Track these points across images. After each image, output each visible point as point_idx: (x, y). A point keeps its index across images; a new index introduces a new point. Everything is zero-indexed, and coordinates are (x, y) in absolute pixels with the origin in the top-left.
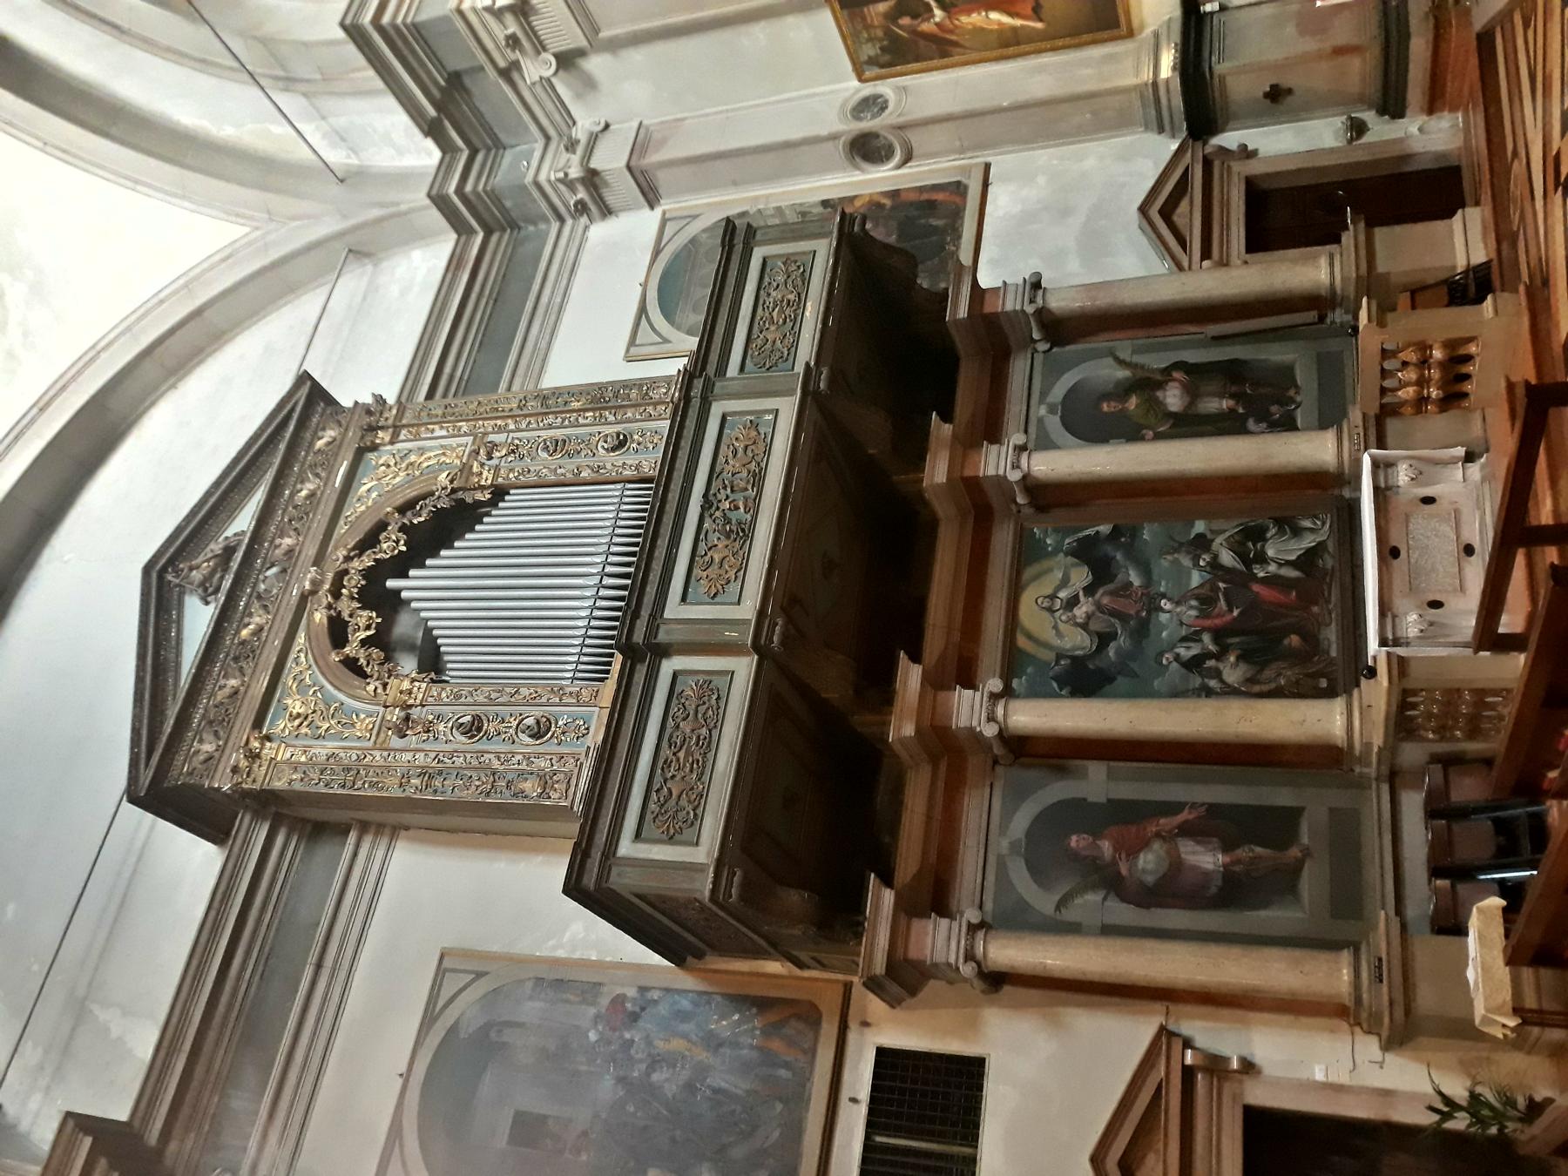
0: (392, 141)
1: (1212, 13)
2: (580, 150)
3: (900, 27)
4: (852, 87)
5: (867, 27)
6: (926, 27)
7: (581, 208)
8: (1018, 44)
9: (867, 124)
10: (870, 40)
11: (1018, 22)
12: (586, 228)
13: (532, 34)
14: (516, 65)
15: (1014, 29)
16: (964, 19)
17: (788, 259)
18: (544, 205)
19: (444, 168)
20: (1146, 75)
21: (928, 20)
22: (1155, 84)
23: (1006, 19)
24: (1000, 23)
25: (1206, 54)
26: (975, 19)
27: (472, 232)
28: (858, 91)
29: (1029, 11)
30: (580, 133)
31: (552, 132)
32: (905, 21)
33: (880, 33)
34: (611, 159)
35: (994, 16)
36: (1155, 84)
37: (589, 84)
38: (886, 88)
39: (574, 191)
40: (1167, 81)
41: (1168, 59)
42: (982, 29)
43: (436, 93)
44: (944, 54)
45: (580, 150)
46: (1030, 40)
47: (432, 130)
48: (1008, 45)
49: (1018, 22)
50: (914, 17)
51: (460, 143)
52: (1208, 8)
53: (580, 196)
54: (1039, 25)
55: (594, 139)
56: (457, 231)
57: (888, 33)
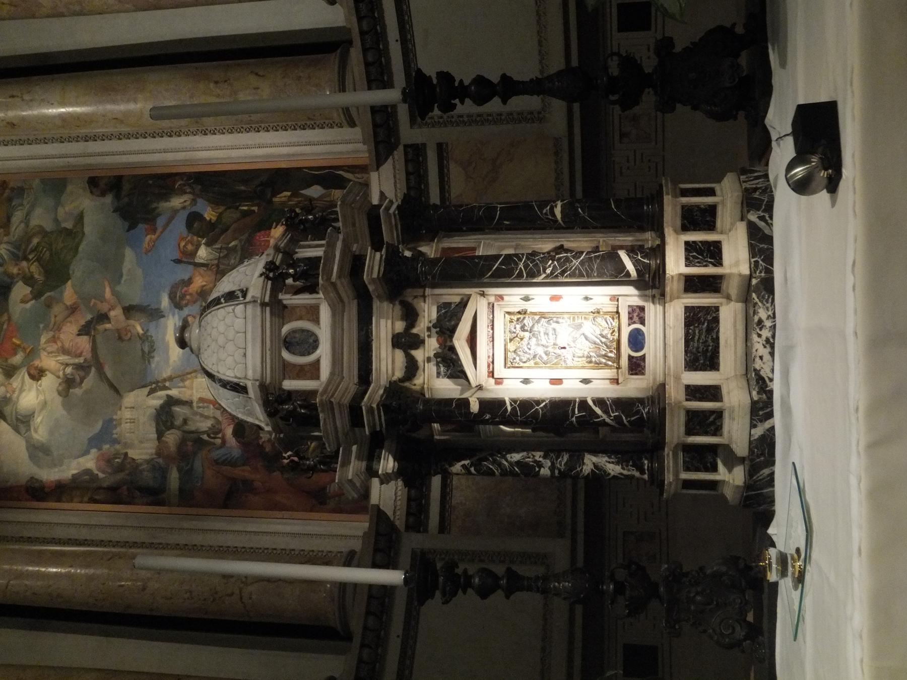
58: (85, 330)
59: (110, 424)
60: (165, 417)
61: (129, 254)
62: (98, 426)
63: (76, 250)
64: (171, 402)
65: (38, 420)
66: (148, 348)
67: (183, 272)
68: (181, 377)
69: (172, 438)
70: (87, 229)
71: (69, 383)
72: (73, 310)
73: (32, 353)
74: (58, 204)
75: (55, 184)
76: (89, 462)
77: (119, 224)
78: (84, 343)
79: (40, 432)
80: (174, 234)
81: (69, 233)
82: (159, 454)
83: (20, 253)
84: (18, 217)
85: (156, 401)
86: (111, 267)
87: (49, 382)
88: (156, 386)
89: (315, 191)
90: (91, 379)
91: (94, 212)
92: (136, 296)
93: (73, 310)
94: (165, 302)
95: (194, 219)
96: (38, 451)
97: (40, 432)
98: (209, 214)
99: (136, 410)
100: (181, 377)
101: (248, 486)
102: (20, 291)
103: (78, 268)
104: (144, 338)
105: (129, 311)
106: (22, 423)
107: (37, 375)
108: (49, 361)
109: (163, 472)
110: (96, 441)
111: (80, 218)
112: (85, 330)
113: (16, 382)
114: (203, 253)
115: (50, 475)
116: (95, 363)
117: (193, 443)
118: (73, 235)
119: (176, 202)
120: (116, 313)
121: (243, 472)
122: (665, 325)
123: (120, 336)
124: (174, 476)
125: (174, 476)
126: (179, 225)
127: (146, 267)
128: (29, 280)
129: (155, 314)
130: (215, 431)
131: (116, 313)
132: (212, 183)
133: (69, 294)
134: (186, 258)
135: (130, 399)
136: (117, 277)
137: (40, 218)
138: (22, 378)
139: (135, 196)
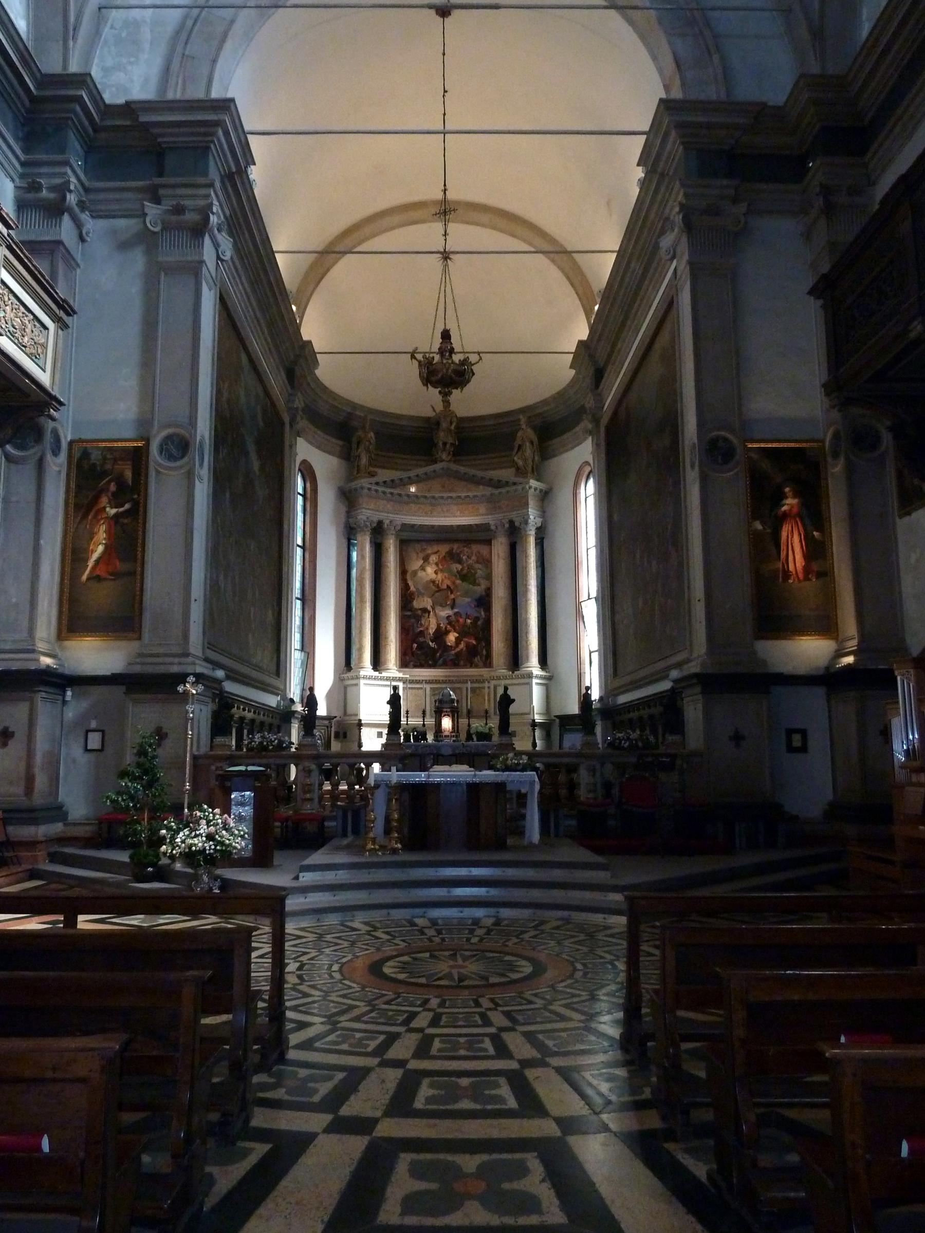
0: (126, 74)
1: (64, 695)
2: (76, 209)
3: (109, 482)
4: (67, 436)
5: (115, 460)
6: (104, 500)
7: (34, 187)
8: (73, 561)
9: (48, 437)
10: (105, 458)
11: (91, 563)
12: (13, 180)
13: (180, 227)
14: (157, 200)
15: (86, 560)
16: (103, 528)
17: (44, 346)
18: (44, 157)
19: (96, 96)
20: (41, 646)
21: (109, 502)
22: (33, 651)
23: (95, 556)
24: (93, 552)
25: (47, 689)
26: (101, 534)
27: (40, 85)
28: (66, 437)
29: (98, 572)
30: (85, 217)
31: (92, 197)
32: (113, 487)
33: (108, 466)
34: (66, 230)
35: (101, 548)
36: (33, 651)
37: (124, 246)
38: (63, 457)
39: (51, 189)
40: (38, 660)
41: (46, 661)
42: (92, 539)
43: (155, 131)
44: (77, 507)
45: (76, 209)
46: (73, 569)
47: (130, 109)
48: (73, 555)
49: (91, 563)
50: (113, 494)
51: (109, 123)
52: (69, 693)
53: (44, 193)
54: (84, 577)
55: (78, 225)
56: (46, 75)
57: (105, 473)
58: (448, 587)
59: (423, 595)
60: (425, 610)
61: (467, 600)
62: (422, 591)
63: (470, 583)
64: (429, 612)
65: (424, 573)
66: (443, 605)
67: (464, 616)
68: (436, 615)
69: (419, 612)
70: (476, 587)
71: (433, 582)
72: (454, 583)
73: (442, 571)
74: (484, 578)
75: (489, 577)
76: (412, 588)
77: (477, 596)
78: (445, 587)
79: (421, 574)
80: (473, 612)
81: (475, 580)
82: (417, 610)
83: (470, 567)
84: (480, 566)
85: (429, 608)
86: (466, 594)
87: (434, 576)
88: (433, 609)
89: (484, 652)
90: (434, 588)
91: (480, 590)
92: (457, 602)
93: (454, 583)
94: (456, 610)
95: (476, 619)
96: (415, 573)
97: (421, 574)
98: (479, 623)
99: (425, 602)
100: (436, 615)
101: (407, 634)
102: (459, 567)
103: (465, 585)
104: (447, 605)
105: (454, 600)
106: (423, 568)
107: (436, 573)
108: (440, 577)
109: (410, 610)
110: (417, 589)
111: (479, 585)
112: (448, 587)
113: (434, 566)
114: (469, 621)
115: (408, 577)
116: (439, 590)
117: (418, 618)
118: (474, 583)
119: (483, 613)
120: (452, 596)
121: (411, 633)
122: (447, 733)
123: (447, 597)
124: (409, 613)
125: (409, 613)
126: (476, 615)
127: (465, 602)
128: (462, 570)
129: (452, 608)
130: (421, 625)
131: (452, 596)
132: (488, 622)
133: (458, 582)
134: (468, 617)
135: (430, 600)
136: (461, 596)
137: (479, 572)
138: (435, 568)
139: (484, 602)
